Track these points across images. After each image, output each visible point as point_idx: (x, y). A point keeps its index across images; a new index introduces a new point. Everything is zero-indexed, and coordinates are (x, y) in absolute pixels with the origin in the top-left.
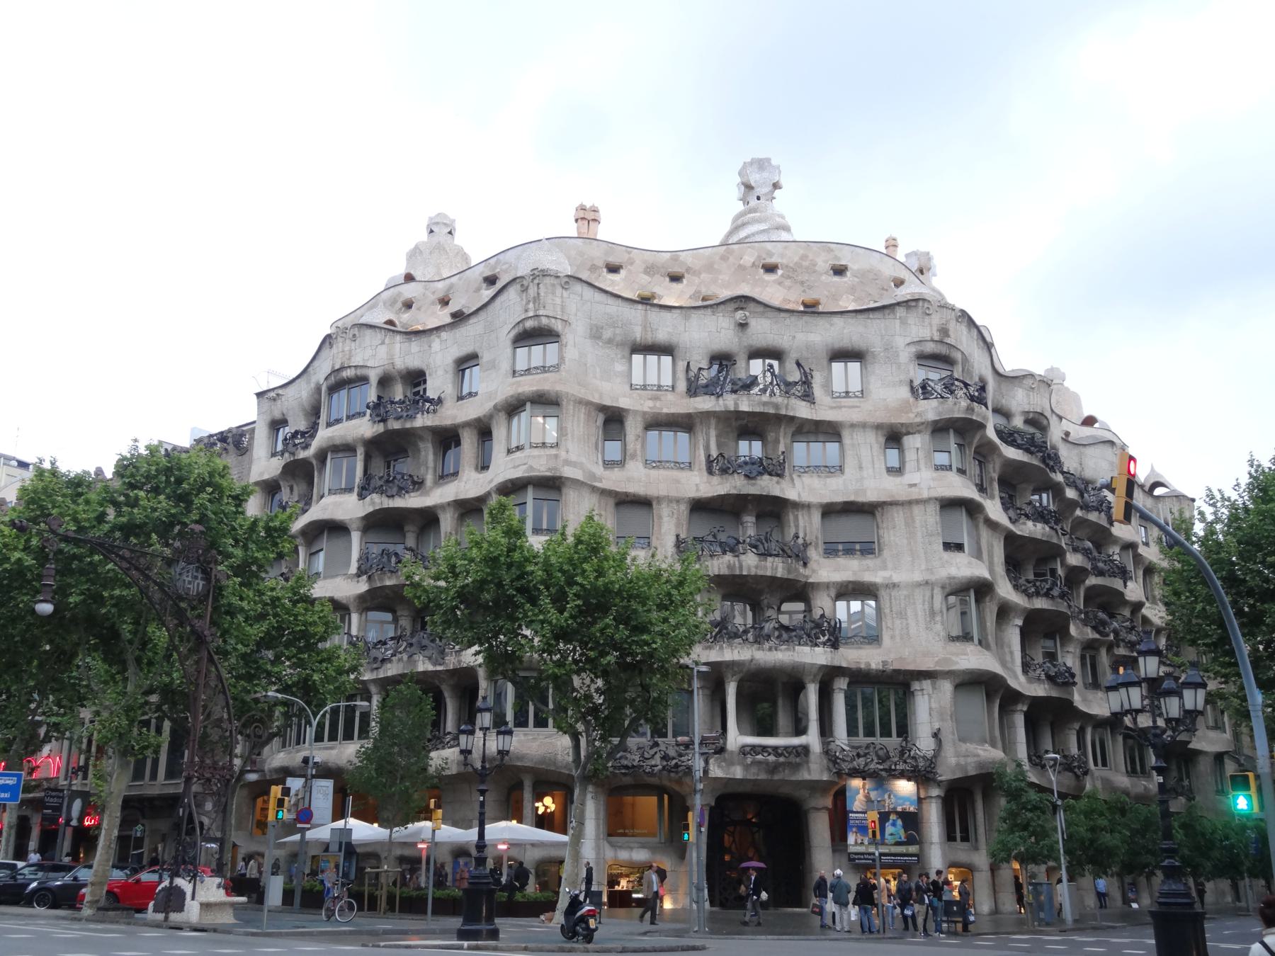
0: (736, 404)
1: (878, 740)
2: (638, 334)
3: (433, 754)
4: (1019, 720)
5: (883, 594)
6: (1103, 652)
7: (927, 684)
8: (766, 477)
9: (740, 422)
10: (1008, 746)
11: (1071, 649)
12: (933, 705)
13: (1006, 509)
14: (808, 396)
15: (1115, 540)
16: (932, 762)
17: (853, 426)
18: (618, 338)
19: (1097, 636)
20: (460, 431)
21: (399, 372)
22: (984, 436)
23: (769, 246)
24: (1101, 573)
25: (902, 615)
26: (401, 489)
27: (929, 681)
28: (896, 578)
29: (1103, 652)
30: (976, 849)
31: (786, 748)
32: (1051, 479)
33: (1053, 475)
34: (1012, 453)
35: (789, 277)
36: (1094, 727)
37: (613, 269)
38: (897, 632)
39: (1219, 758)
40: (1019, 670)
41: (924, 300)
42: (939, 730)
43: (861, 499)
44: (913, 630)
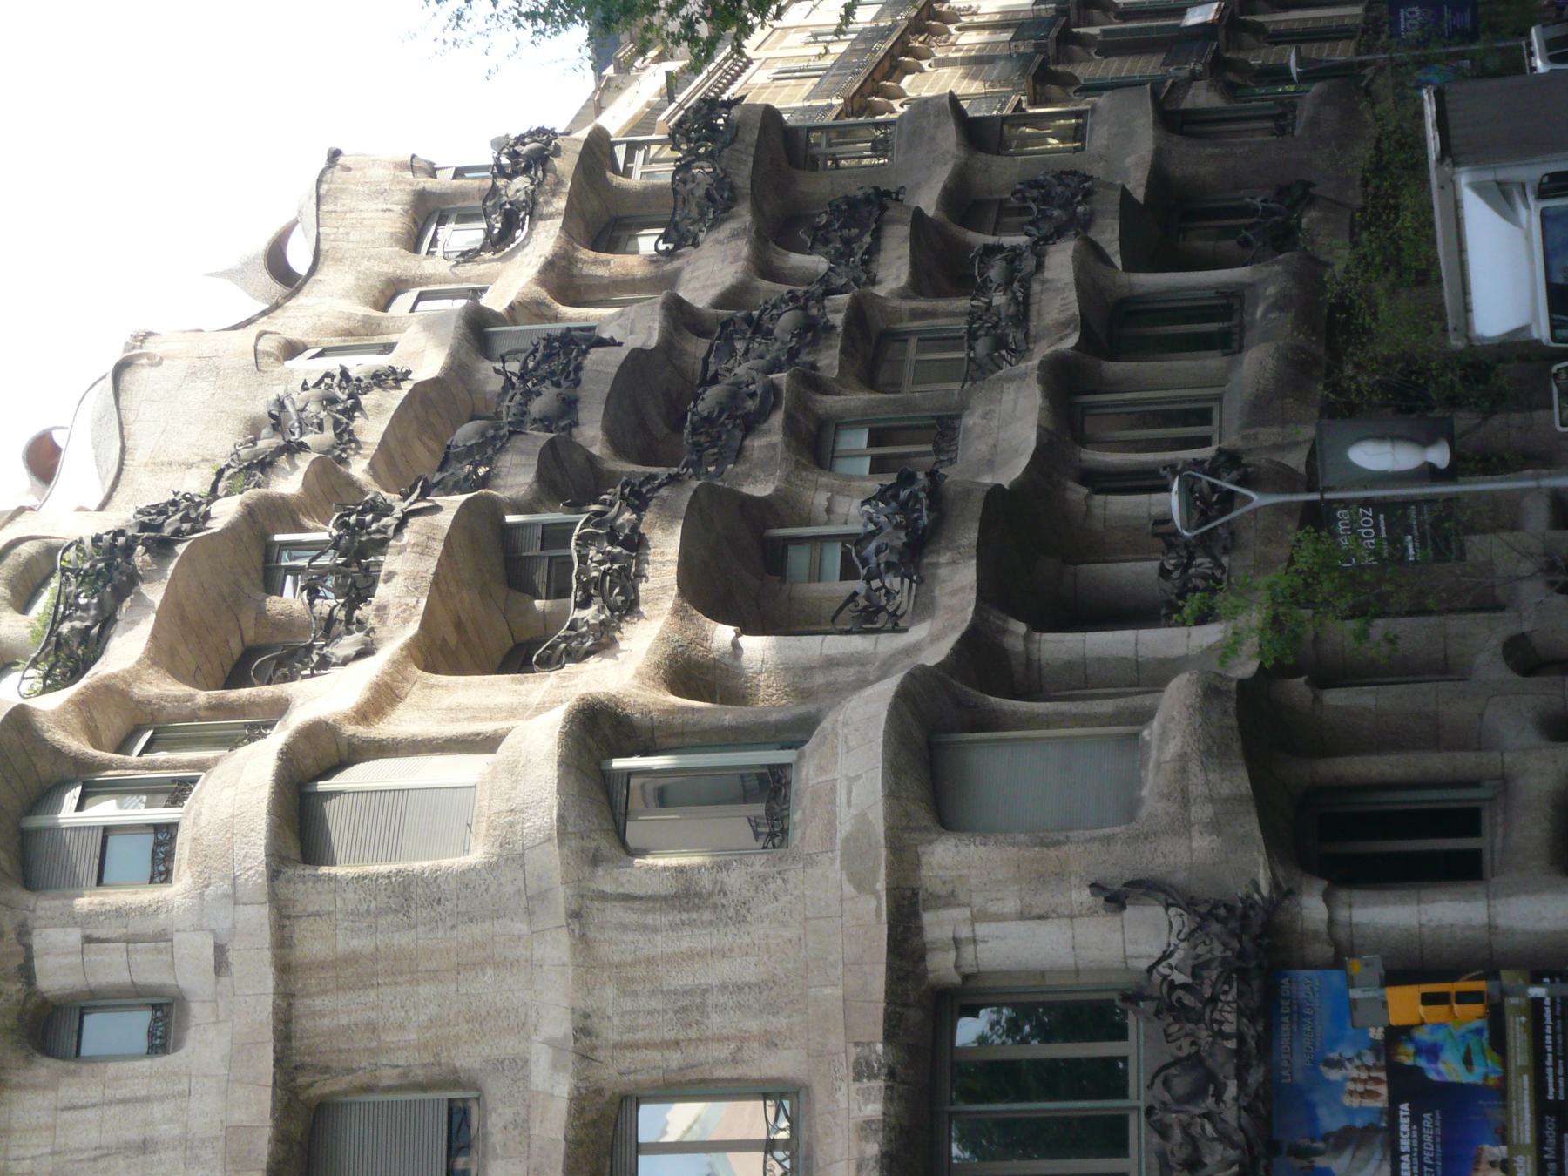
1: (1139, 1094)
4: (1058, 646)
5: (613, 1072)
6: (830, 403)
7: (937, 925)
10: (1150, 677)
11: (821, 499)
12: (1011, 905)
13: (325, 663)
15: (457, 371)
16: (1204, 910)
19: (777, 419)
22: (59, 718)
24: (569, 406)
25: (691, 1005)
27: (928, 918)
28: (557, 1024)
29: (830, 403)
30: (1505, 782)
32: (231, 530)
33: (216, 526)
34: (126, 650)
36: (1084, 441)
38: (753, 1025)
39: (1172, 119)
40: (889, 643)
42: (1096, 888)
44: (746, 970)
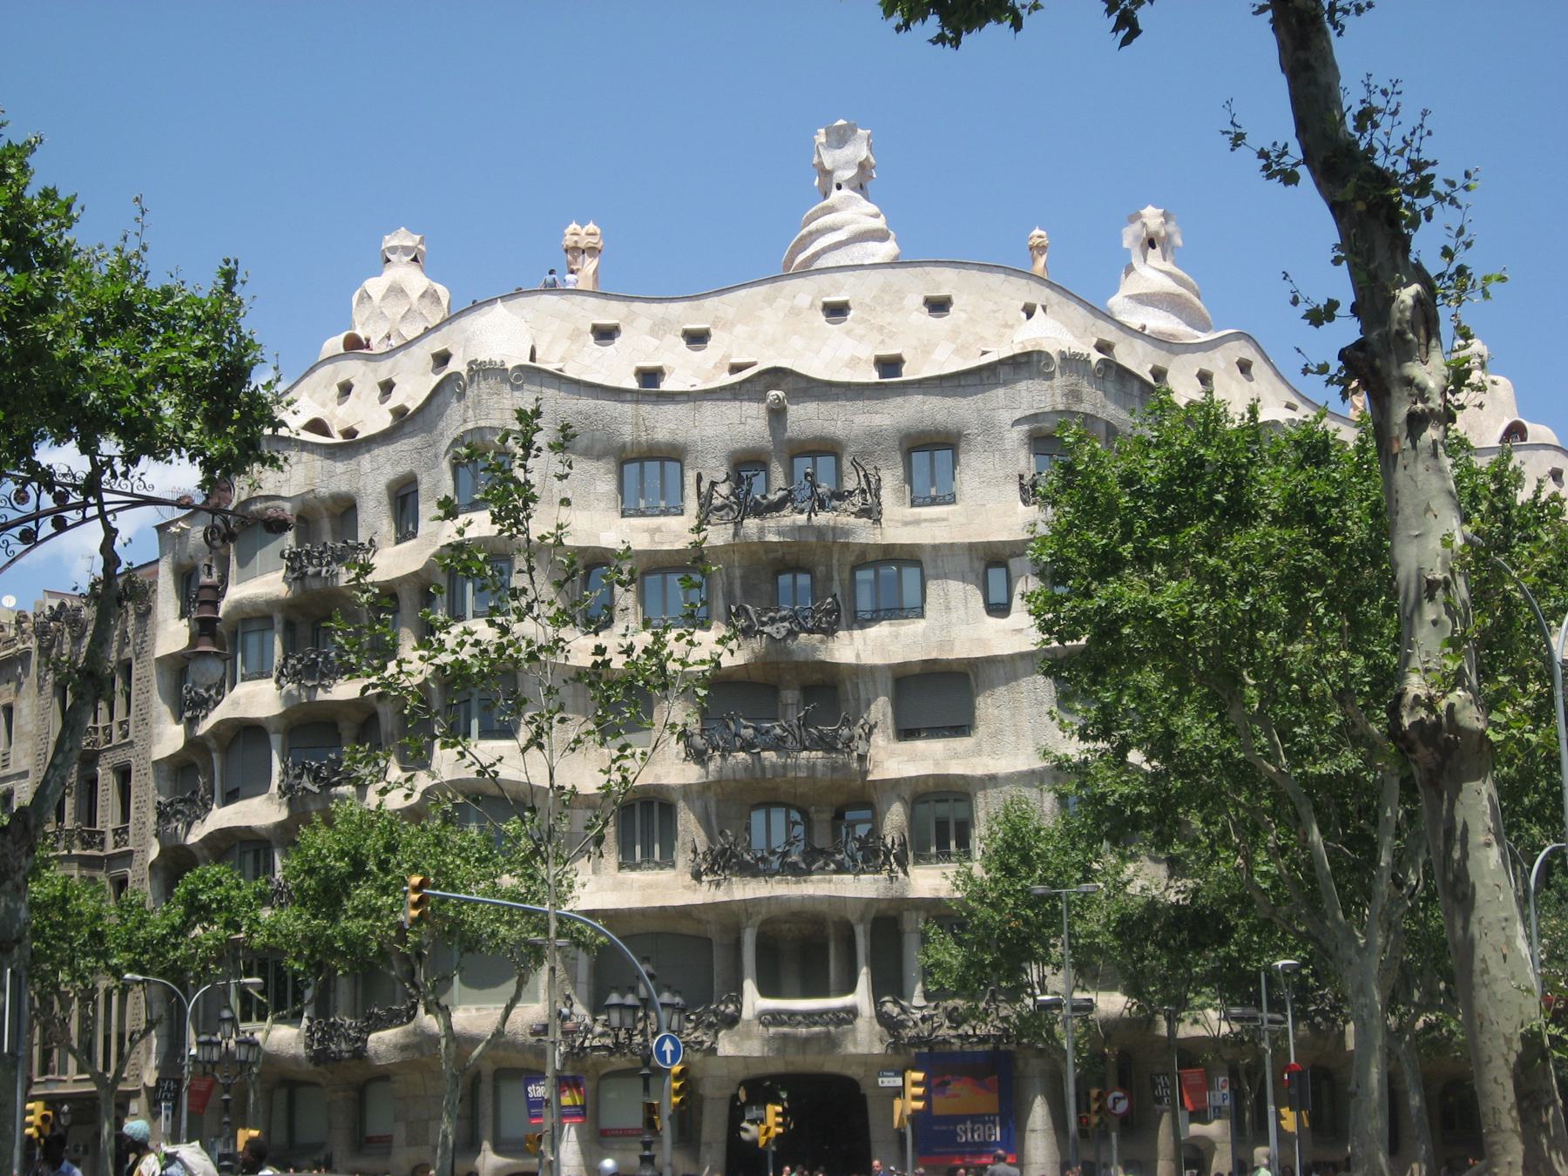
0: (762, 530)
2: (627, 434)
3: (373, 1037)
8: (803, 636)
9: (772, 556)
14: (871, 512)
17: (936, 548)
18: (598, 447)
20: (398, 590)
21: (322, 500)
23: (838, 276)
26: (324, 676)
31: (822, 1013)
35: (863, 321)
37: (605, 334)
41: (1040, 352)
43: (944, 656)
